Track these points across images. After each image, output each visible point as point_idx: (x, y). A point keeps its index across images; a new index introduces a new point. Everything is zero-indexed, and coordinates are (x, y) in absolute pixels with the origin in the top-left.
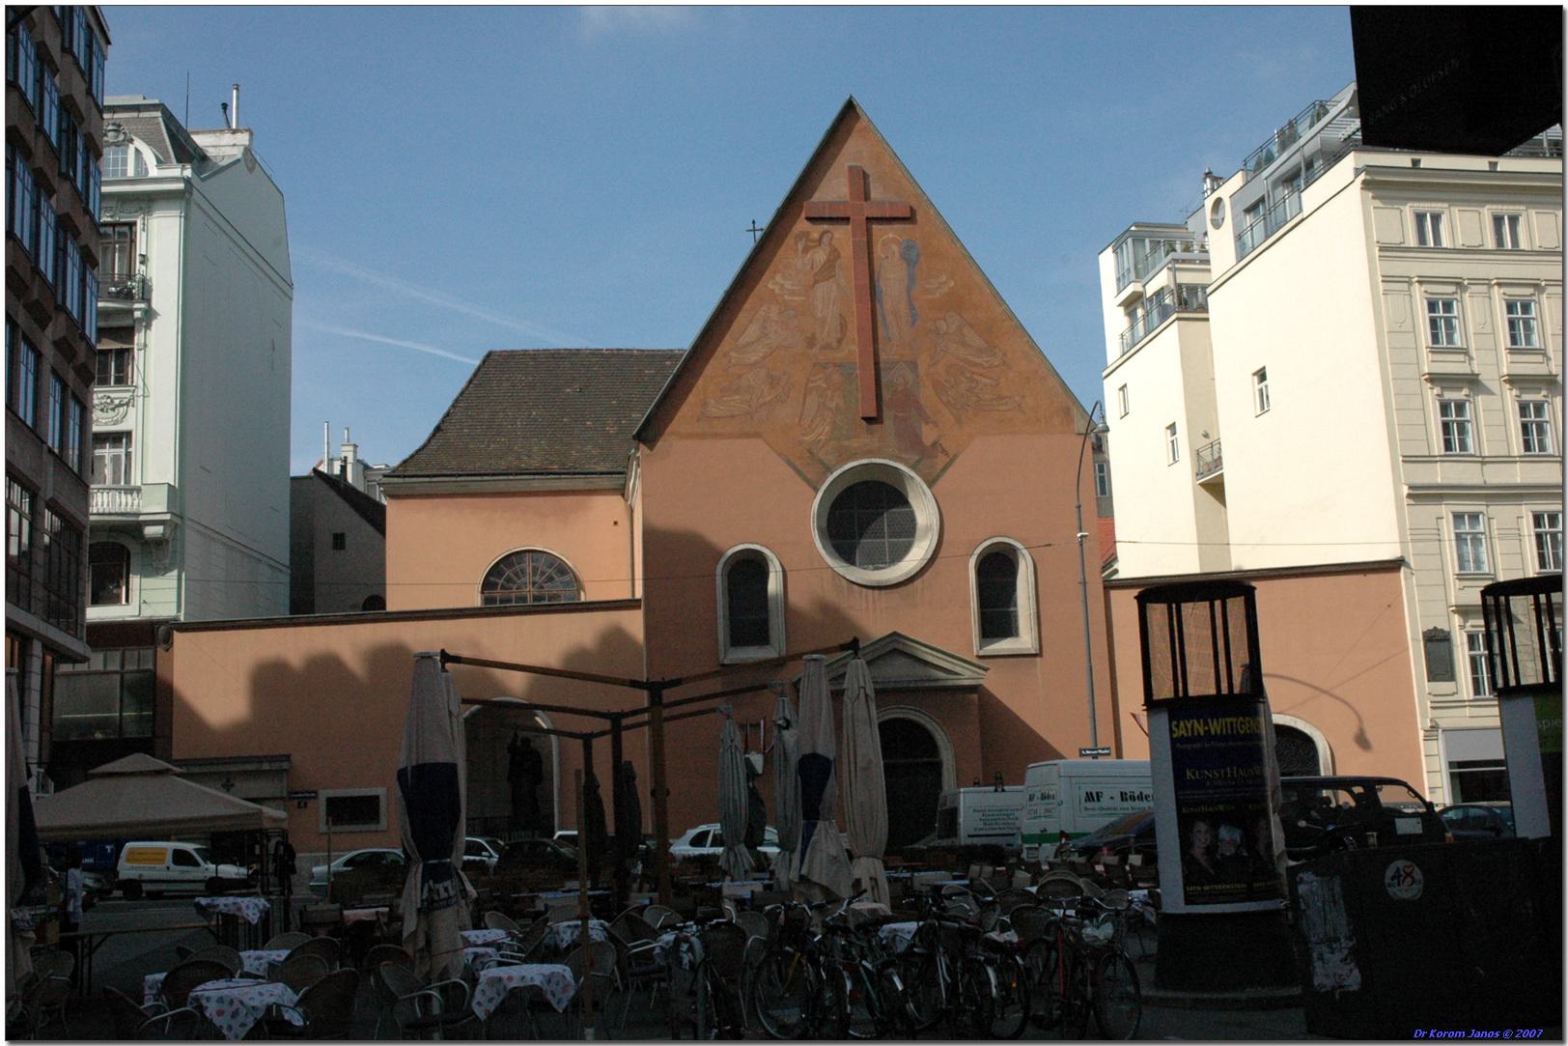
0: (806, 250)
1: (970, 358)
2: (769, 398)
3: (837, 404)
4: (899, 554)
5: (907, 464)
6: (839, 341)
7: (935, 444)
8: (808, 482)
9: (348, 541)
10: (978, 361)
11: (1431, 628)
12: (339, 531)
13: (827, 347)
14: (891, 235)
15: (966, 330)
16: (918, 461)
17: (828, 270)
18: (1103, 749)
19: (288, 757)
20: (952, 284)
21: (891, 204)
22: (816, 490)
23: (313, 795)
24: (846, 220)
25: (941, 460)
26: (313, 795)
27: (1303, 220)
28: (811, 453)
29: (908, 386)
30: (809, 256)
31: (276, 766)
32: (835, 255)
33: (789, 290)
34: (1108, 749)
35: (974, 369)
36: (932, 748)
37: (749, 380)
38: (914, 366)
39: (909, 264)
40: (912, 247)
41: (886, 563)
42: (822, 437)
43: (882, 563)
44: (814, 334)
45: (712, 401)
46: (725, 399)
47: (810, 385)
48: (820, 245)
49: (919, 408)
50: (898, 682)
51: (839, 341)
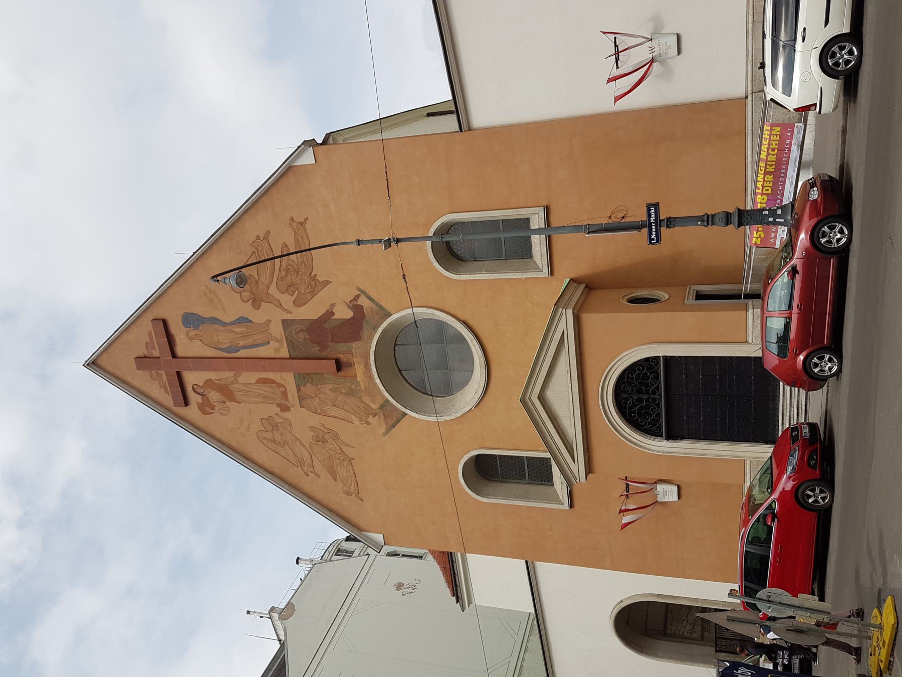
3: (331, 390)
8: (398, 421)
18: (650, 216)
22: (405, 414)
24: (179, 374)
25: (363, 301)
29: (304, 329)
32: (209, 383)
34: (649, 210)
36: (649, 363)
37: (324, 459)
48: (204, 395)
51: (279, 385)
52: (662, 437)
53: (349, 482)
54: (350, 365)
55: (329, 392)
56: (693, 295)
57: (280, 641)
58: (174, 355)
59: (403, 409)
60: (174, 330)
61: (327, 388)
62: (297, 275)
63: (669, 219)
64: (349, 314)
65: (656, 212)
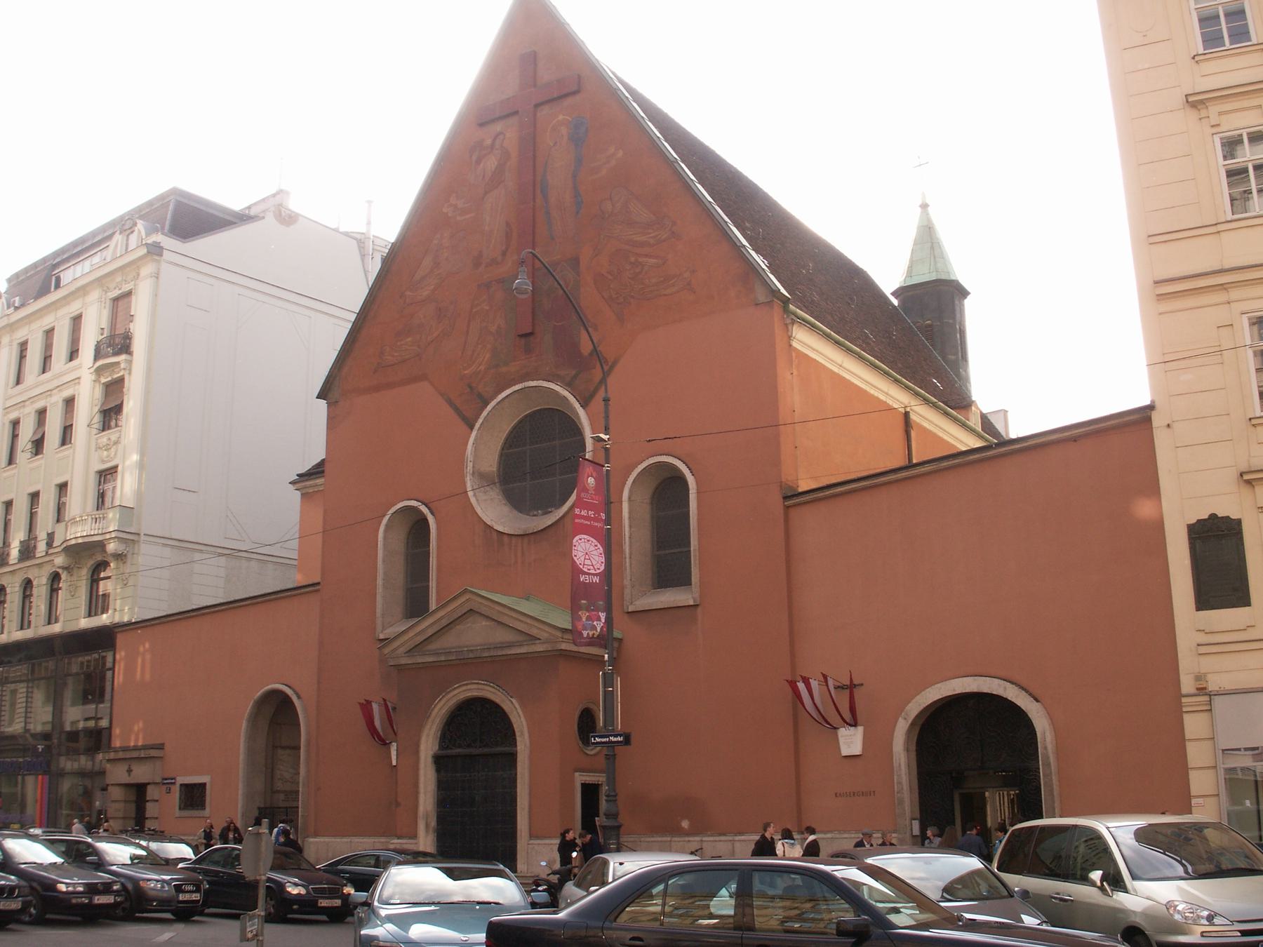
6: (504, 254)
10: (643, 238)
11: (1205, 515)
14: (561, 117)
16: (575, 377)
18: (616, 736)
22: (472, 428)
23: (173, 781)
26: (173, 781)
30: (482, 165)
38: (575, 262)
42: (482, 368)
46: (399, 344)
50: (472, 651)
52: (440, 749)
53: (396, 354)
56: (591, 778)
57: (249, 208)
59: (477, 425)
60: (569, 101)
62: (629, 278)
65: (618, 742)
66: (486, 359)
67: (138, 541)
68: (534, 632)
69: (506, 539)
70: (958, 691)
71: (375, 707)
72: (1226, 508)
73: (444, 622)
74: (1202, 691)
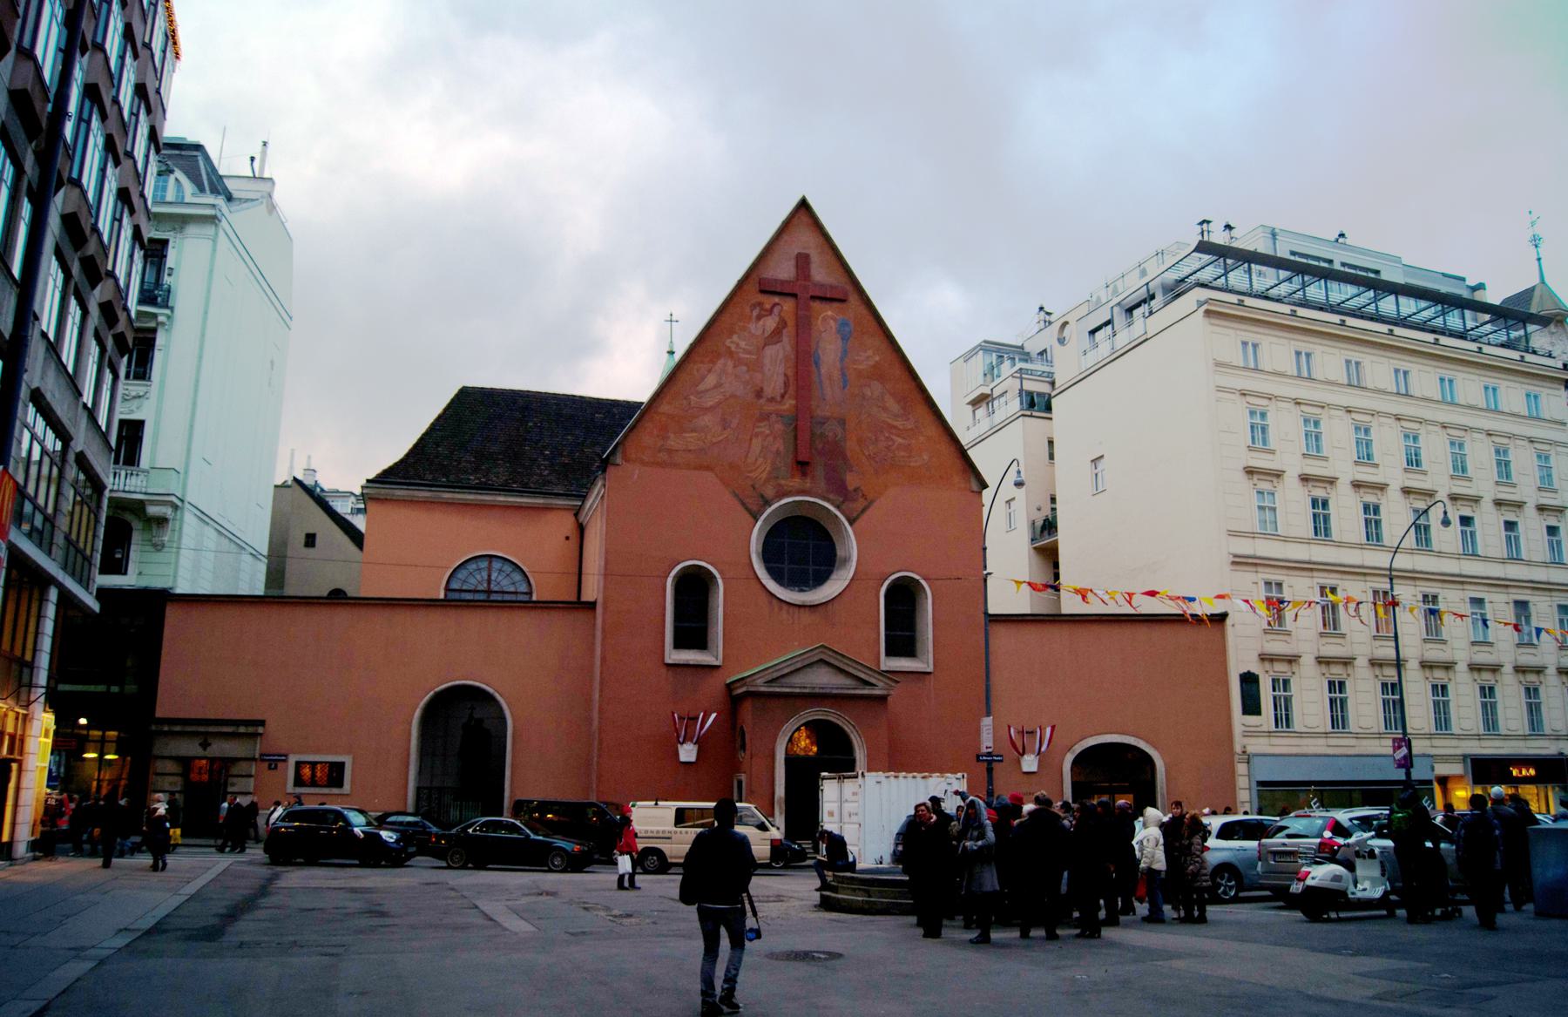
0: (759, 318)
1: (890, 421)
2: (721, 438)
4: (821, 579)
5: (832, 504)
6: (783, 396)
7: (855, 490)
8: (749, 511)
9: (318, 541)
10: (895, 423)
11: (1246, 671)
12: (311, 531)
13: (772, 400)
14: (830, 313)
15: (887, 397)
16: (843, 502)
17: (776, 334)
18: (997, 756)
19: (262, 723)
20: (877, 358)
21: (832, 287)
23: (283, 758)
26: (283, 758)
27: (1147, 340)
28: (754, 488)
30: (761, 323)
31: (251, 730)
33: (744, 349)
35: (894, 431)
38: (842, 422)
39: (843, 339)
40: (847, 324)
41: (809, 586)
42: (764, 475)
43: (806, 587)
44: (762, 389)
45: (672, 436)
46: (684, 435)
47: (757, 430)
49: (845, 458)
50: (822, 688)
51: (783, 396)
54: (804, 474)
55: (776, 446)
58: (813, 298)
61: (779, 445)
63: (992, 769)
64: (851, 488)
66: (767, 469)
67: (182, 509)
68: (873, 680)
69: (785, 607)
70: (1109, 741)
71: (676, 715)
72: (1255, 668)
73: (799, 665)
74: (1244, 752)
